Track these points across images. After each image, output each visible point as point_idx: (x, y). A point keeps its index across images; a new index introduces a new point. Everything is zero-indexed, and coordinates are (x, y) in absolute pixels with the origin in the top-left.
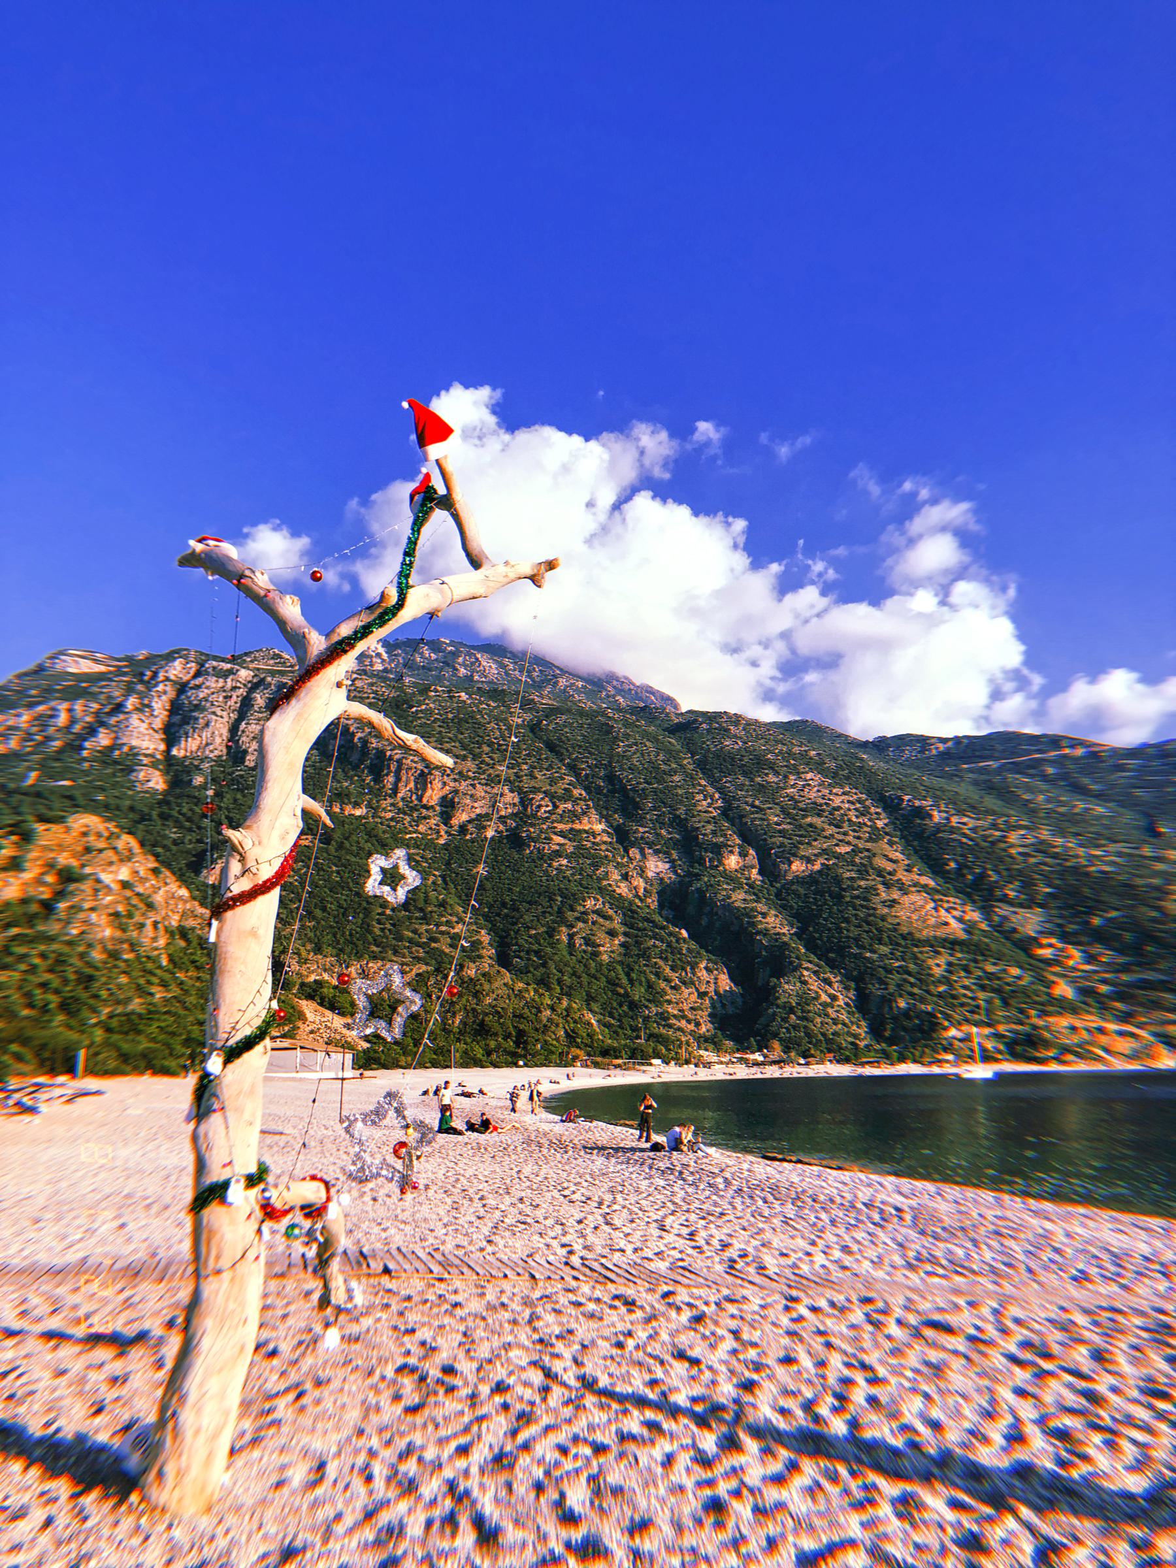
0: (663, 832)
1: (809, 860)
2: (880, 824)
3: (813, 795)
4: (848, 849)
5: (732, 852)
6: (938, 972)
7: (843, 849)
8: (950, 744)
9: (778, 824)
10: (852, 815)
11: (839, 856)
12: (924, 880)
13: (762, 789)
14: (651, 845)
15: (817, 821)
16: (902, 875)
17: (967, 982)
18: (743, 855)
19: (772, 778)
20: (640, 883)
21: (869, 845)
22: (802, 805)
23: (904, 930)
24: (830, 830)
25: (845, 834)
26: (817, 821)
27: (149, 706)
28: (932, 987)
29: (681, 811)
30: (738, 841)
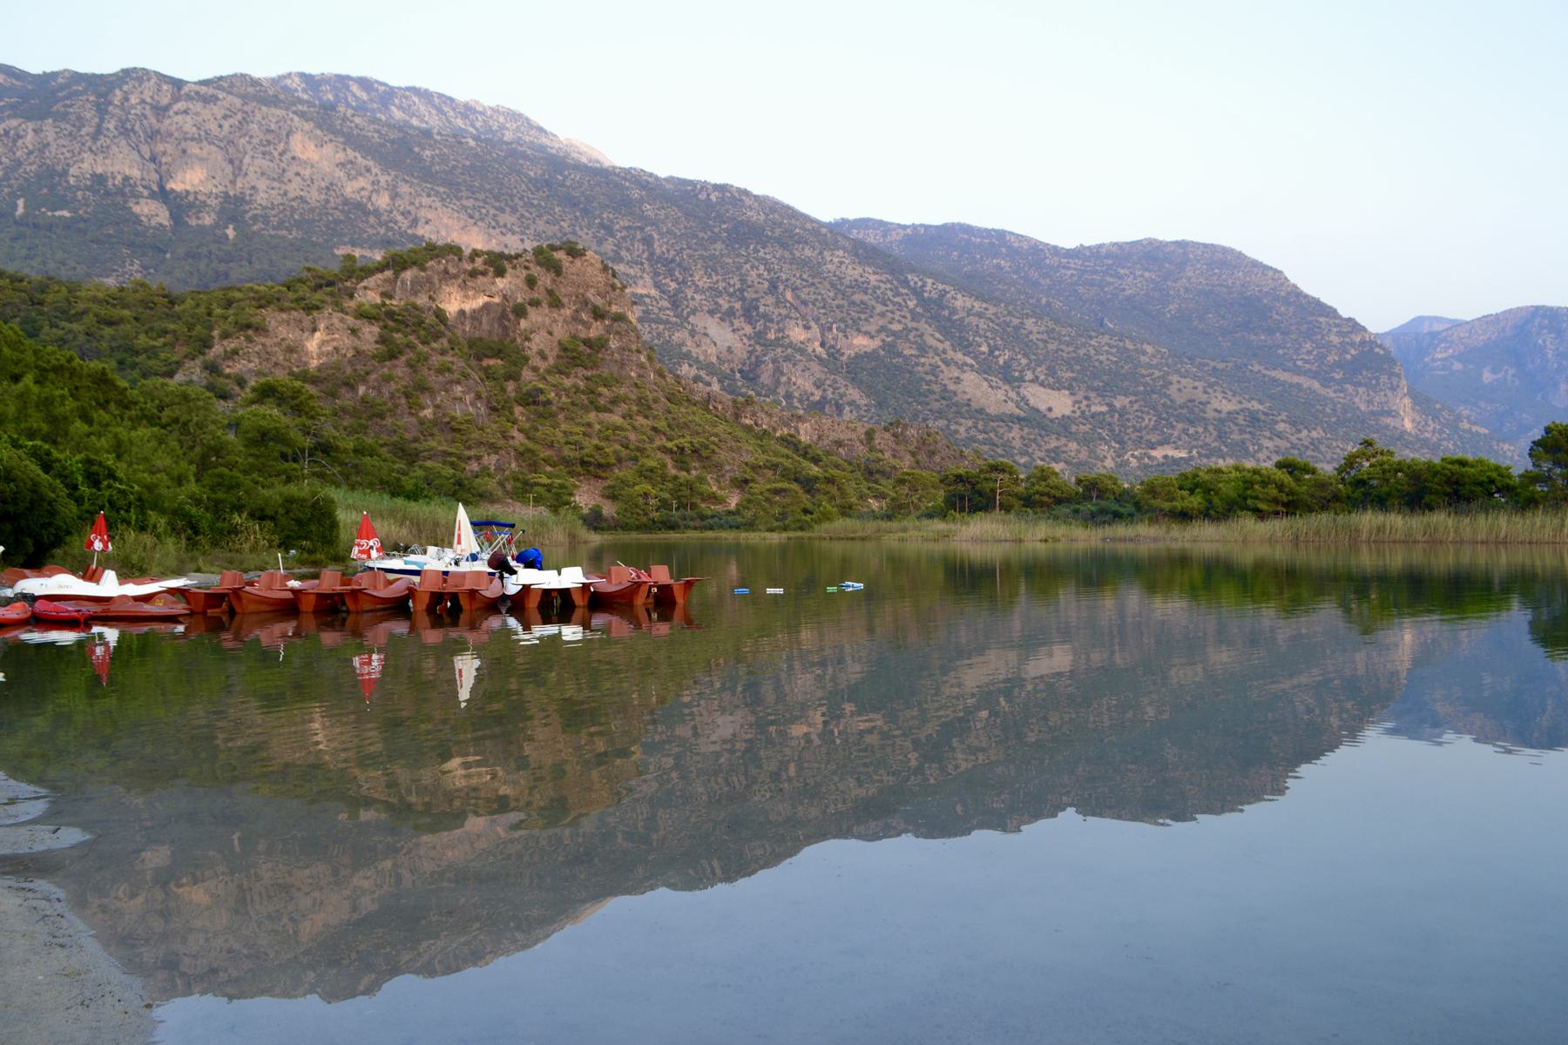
0: (720, 301)
1: (872, 337)
2: (911, 304)
6: (1017, 443)
7: (896, 327)
11: (894, 334)
12: (969, 361)
13: (804, 263)
14: (711, 313)
15: (865, 298)
16: (951, 354)
17: (1042, 454)
20: (712, 350)
21: (914, 325)
23: (974, 405)
24: (880, 308)
26: (865, 298)
27: (132, 130)
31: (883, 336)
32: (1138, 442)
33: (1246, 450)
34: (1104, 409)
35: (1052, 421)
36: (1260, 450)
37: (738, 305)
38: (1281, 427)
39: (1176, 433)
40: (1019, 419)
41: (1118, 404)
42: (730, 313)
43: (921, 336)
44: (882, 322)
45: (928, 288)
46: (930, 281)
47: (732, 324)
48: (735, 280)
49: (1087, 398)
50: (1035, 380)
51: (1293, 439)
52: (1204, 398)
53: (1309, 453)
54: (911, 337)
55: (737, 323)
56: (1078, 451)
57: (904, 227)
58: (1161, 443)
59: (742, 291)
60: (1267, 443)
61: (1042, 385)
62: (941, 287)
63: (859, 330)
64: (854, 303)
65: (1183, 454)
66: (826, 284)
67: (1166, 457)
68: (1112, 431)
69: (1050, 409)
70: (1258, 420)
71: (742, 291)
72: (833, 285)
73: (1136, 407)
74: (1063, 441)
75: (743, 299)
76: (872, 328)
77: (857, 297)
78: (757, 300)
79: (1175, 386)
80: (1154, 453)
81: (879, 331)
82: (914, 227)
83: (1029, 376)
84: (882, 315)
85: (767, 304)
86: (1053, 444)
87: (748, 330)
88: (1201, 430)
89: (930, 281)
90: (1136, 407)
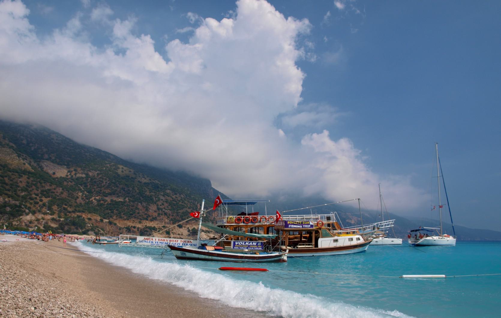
28: (19, 192)
32: (99, 193)
33: (152, 199)
34: (84, 176)
35: (54, 179)
36: (159, 200)
38: (168, 191)
39: (118, 190)
40: (29, 173)
41: (90, 174)
49: (75, 170)
50: (49, 159)
51: (174, 197)
52: (134, 176)
53: (180, 203)
56: (62, 193)
58: (110, 194)
60: (162, 198)
61: (53, 162)
65: (121, 200)
67: (112, 200)
68: (86, 186)
69: (54, 173)
70: (158, 187)
73: (100, 176)
74: (54, 186)
79: (121, 170)
80: (107, 198)
83: (46, 156)
86: (47, 187)
88: (131, 189)
90: (100, 176)
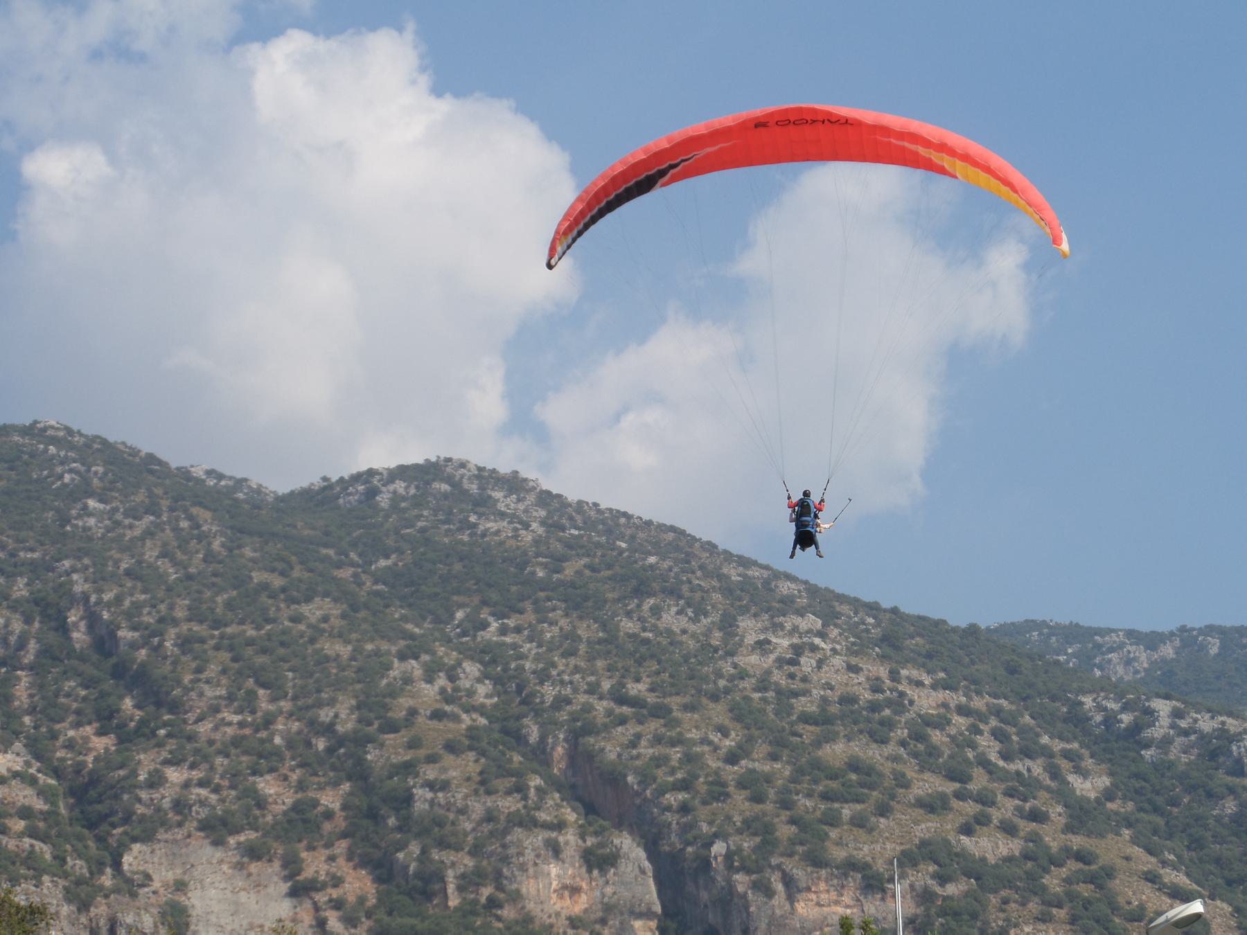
0: (268, 786)
1: (874, 884)
3: (835, 673)
4: (1014, 846)
5: (556, 850)
7: (990, 847)
8: (1168, 651)
9: (732, 759)
10: (988, 745)
15: (874, 754)
18: (599, 861)
19: (671, 619)
22: (805, 705)
25: (984, 799)
29: (342, 714)
30: (571, 816)
31: (923, 876)
37: (330, 799)
42: (304, 821)
43: (1102, 877)
44: (927, 827)
45: (1158, 731)
46: (1163, 707)
47: (292, 866)
48: (342, 714)
54: (1053, 882)
55: (315, 865)
57: (1152, 641)
59: (360, 741)
62: (1207, 724)
63: (816, 861)
64: (818, 768)
66: (718, 712)
71: (360, 741)
72: (740, 713)
75: (360, 774)
76: (878, 850)
77: (837, 752)
78: (408, 768)
81: (908, 860)
82: (1187, 637)
84: (933, 805)
85: (451, 785)
87: (358, 884)
89: (1163, 707)
